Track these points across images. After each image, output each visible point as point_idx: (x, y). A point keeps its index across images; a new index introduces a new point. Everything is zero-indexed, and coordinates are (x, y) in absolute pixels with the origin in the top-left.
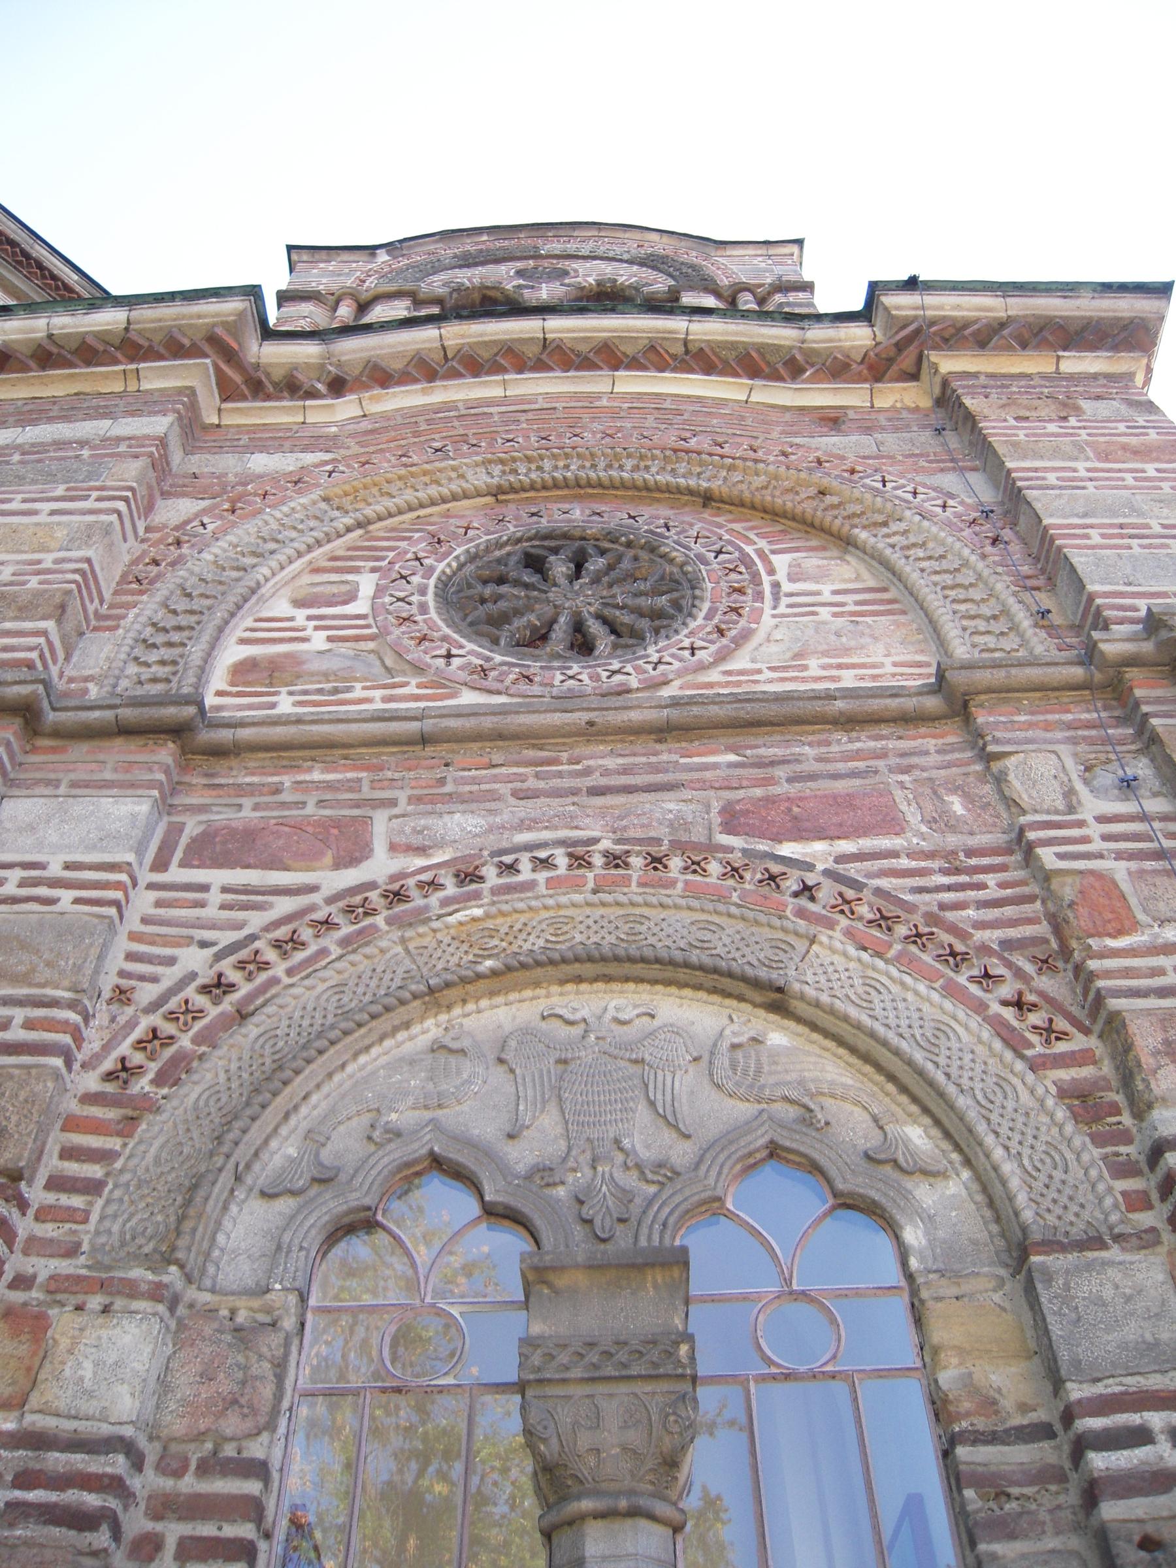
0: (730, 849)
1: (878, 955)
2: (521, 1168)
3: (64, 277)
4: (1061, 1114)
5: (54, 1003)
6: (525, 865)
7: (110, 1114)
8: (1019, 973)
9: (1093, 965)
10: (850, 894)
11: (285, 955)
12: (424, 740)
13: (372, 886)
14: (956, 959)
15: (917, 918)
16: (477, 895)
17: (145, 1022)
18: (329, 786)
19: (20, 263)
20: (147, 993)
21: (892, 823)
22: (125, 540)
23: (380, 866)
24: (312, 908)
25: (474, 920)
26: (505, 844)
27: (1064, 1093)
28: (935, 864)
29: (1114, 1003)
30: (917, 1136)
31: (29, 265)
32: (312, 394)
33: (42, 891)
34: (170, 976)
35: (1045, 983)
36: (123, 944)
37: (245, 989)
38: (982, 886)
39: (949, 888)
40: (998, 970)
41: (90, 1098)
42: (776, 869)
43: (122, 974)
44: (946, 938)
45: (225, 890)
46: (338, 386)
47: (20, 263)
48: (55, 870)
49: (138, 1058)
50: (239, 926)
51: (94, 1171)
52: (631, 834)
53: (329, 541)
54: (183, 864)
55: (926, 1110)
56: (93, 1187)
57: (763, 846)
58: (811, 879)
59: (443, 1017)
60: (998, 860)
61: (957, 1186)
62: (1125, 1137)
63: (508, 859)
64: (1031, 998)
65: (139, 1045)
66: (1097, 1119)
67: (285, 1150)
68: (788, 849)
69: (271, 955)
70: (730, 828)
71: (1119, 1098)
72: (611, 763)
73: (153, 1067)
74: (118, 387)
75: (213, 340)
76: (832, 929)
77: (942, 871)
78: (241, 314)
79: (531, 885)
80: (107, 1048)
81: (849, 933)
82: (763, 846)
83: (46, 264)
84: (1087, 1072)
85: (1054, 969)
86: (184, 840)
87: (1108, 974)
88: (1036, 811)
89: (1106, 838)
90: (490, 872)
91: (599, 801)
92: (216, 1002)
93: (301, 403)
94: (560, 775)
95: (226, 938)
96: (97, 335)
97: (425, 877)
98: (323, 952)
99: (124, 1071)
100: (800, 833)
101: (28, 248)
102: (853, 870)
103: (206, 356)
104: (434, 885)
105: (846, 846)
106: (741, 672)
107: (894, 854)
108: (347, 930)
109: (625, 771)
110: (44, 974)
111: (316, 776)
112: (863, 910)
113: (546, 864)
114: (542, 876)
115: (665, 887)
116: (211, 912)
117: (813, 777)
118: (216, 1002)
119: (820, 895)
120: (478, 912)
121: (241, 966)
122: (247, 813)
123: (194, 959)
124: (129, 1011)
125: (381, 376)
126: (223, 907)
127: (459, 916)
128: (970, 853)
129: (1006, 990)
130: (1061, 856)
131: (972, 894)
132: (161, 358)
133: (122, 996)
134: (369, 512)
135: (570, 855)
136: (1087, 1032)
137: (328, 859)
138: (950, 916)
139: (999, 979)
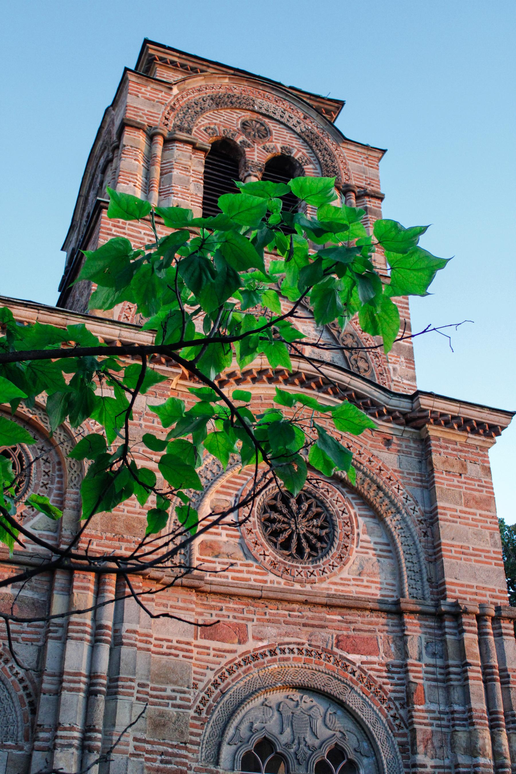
0: (337, 654)
2: (284, 743)
4: (397, 750)
5: (184, 692)
6: (287, 651)
7: (198, 723)
8: (396, 708)
9: (414, 713)
10: (363, 675)
11: (230, 674)
13: (248, 652)
14: (383, 701)
15: (377, 686)
16: (275, 661)
17: (203, 694)
18: (235, 610)
21: (375, 652)
23: (251, 645)
24: (235, 659)
26: (281, 641)
27: (400, 744)
29: (416, 726)
30: (365, 744)
33: (173, 651)
34: (206, 679)
35: (402, 712)
37: (223, 685)
39: (386, 677)
40: (392, 706)
41: (194, 718)
43: (194, 679)
44: (382, 693)
45: (214, 649)
48: (174, 644)
49: (201, 706)
50: (219, 664)
51: (198, 739)
52: (313, 643)
54: (201, 638)
55: (369, 739)
56: (198, 744)
57: (345, 654)
58: (355, 669)
60: (399, 670)
61: (372, 760)
62: (408, 758)
63: (282, 647)
64: (397, 716)
65: (200, 702)
66: (404, 753)
67: (231, 731)
68: (351, 657)
69: (227, 674)
70: (337, 647)
71: (409, 747)
72: (310, 614)
73: (205, 709)
79: (287, 659)
82: (345, 654)
84: (404, 739)
85: (404, 708)
87: (417, 717)
89: (426, 672)
90: (278, 651)
91: (306, 629)
92: (216, 688)
94: (296, 616)
97: (261, 651)
98: (239, 675)
100: (355, 651)
102: (365, 667)
104: (264, 655)
105: (364, 658)
106: (346, 579)
107: (374, 663)
108: (244, 668)
109: (312, 619)
110: (181, 682)
111: (231, 605)
112: (365, 680)
113: (292, 651)
114: (291, 656)
116: (211, 658)
117: (360, 630)
118: (216, 688)
119: (357, 674)
121: (220, 677)
123: (210, 676)
124: (198, 691)
126: (214, 656)
128: (393, 666)
129: (392, 713)
130: (415, 677)
133: (195, 686)
135: (298, 649)
136: (407, 728)
137: (237, 640)
139: (391, 709)
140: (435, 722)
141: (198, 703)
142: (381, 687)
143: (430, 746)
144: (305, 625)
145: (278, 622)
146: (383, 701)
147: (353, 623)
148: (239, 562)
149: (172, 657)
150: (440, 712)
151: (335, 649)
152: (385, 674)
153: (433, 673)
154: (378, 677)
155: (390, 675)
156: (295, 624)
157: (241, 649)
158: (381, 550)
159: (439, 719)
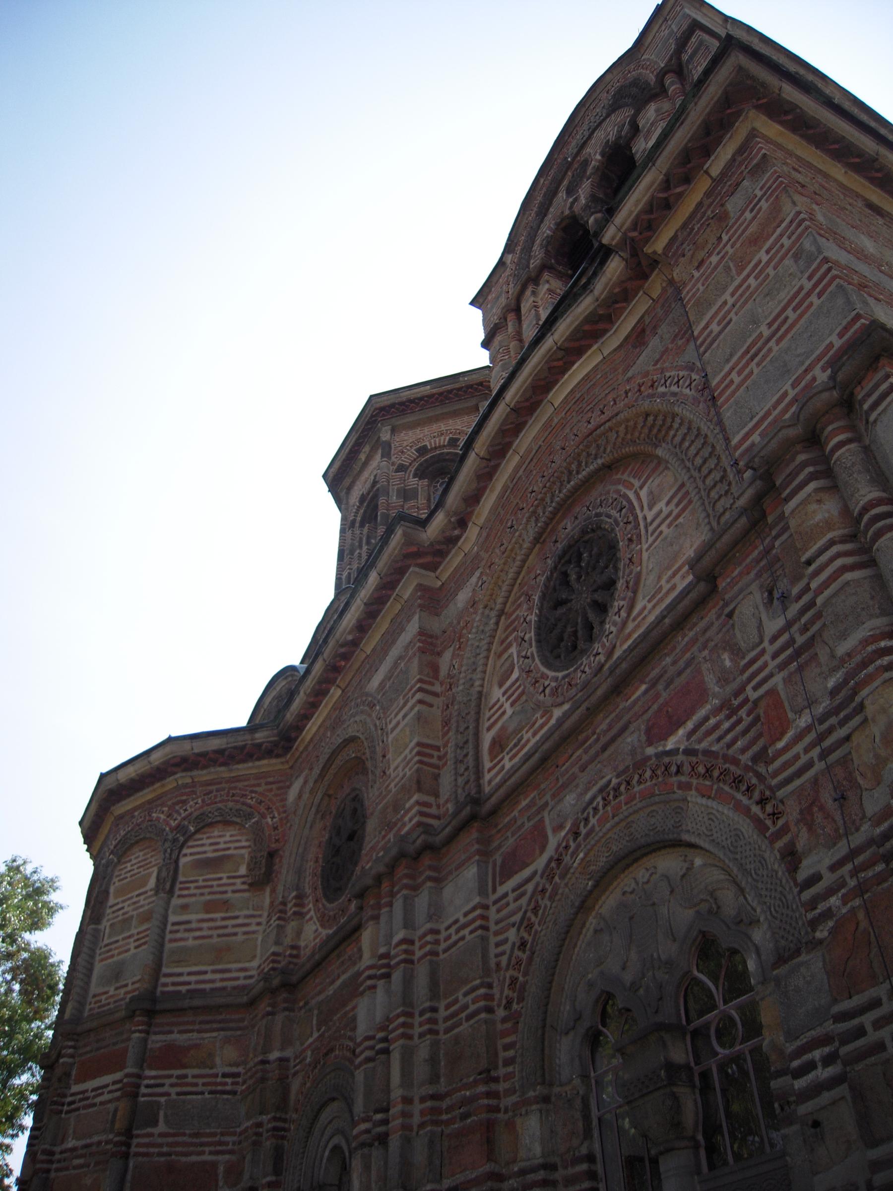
1: (709, 797)
3: (426, 393)
12: (544, 760)
19: (403, 410)
20: (504, 960)
21: (703, 695)
22: (431, 706)
24: (537, 884)
25: (583, 859)
28: (721, 716)
31: (406, 406)
32: (458, 538)
34: (507, 947)
36: (493, 940)
38: (740, 721)
42: (667, 760)
44: (733, 768)
46: (462, 523)
47: (403, 410)
53: (494, 637)
58: (680, 758)
59: (594, 913)
68: (670, 745)
74: (399, 607)
75: (406, 556)
76: (691, 790)
77: (728, 717)
78: (405, 534)
80: (502, 992)
81: (697, 789)
83: (412, 397)
86: (498, 869)
88: (749, 651)
93: (456, 548)
94: (590, 747)
95: (517, 918)
96: (376, 589)
97: (564, 844)
98: (546, 907)
99: (509, 1003)
101: (400, 400)
103: (409, 567)
107: (706, 719)
111: (524, 803)
115: (632, 801)
120: (581, 855)
122: (511, 841)
124: (502, 973)
125: (473, 499)
127: (577, 861)
129: (756, 795)
130: (755, 689)
131: (739, 728)
132: (399, 581)
134: (498, 607)
138: (731, 752)
140: (815, 752)
141: (506, 992)
142: (726, 758)
143: (819, 817)
144: (604, 748)
145: (574, 777)
146: (737, 781)
147: (662, 676)
148: (524, 732)
149: (461, 943)
150: (821, 721)
151: (650, 751)
152: (726, 725)
153: (792, 641)
154: (719, 739)
155: (734, 718)
156: (592, 760)
157: (540, 863)
158: (677, 505)
159: (821, 738)
